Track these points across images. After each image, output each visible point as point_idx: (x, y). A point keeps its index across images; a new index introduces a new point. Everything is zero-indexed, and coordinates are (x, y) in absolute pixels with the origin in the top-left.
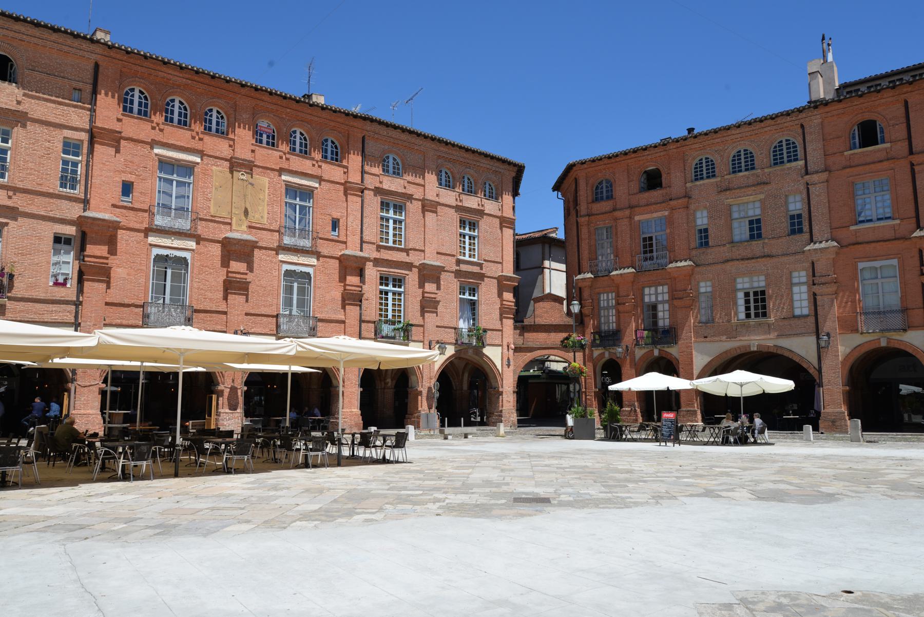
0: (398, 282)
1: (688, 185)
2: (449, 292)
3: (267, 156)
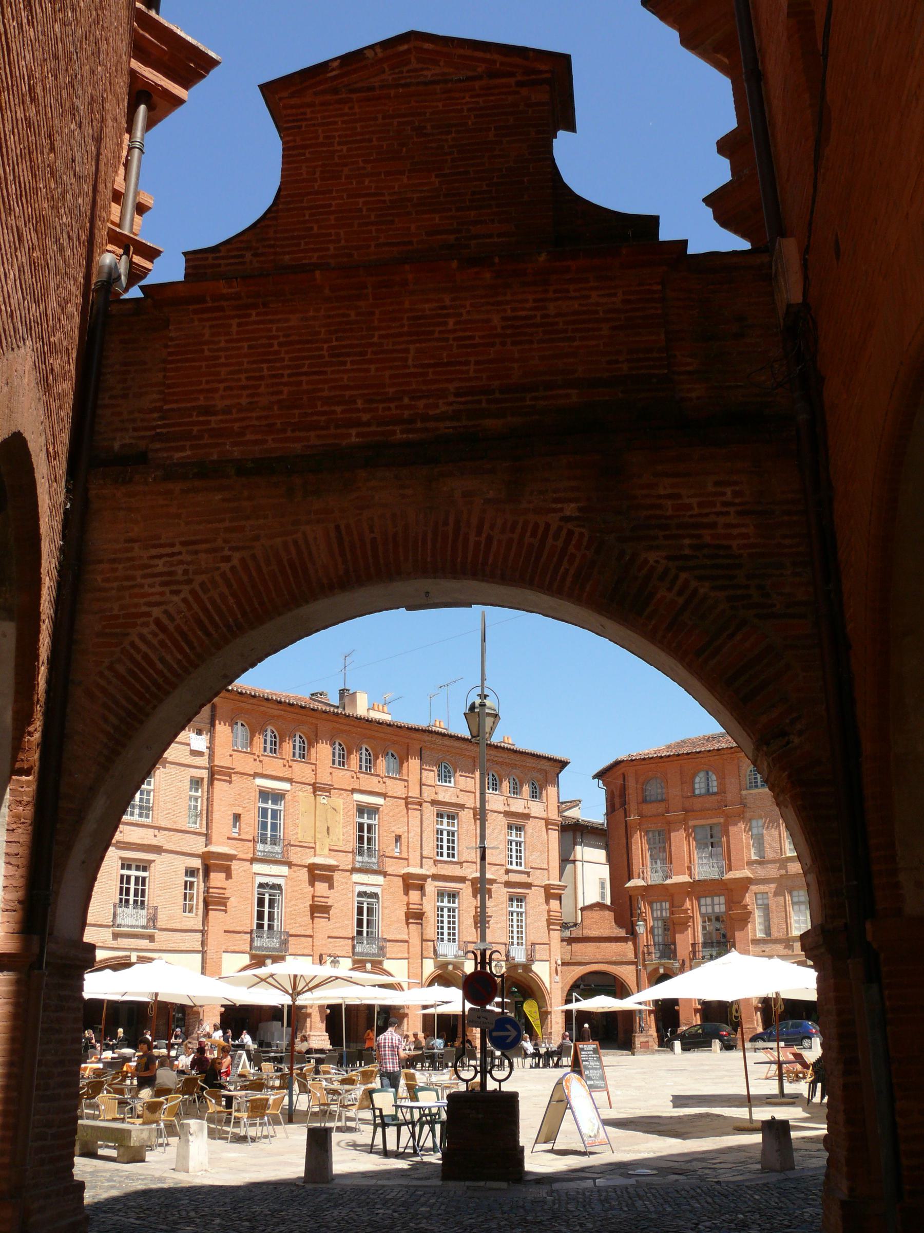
0: (453, 896)
1: (744, 792)
3: (342, 777)
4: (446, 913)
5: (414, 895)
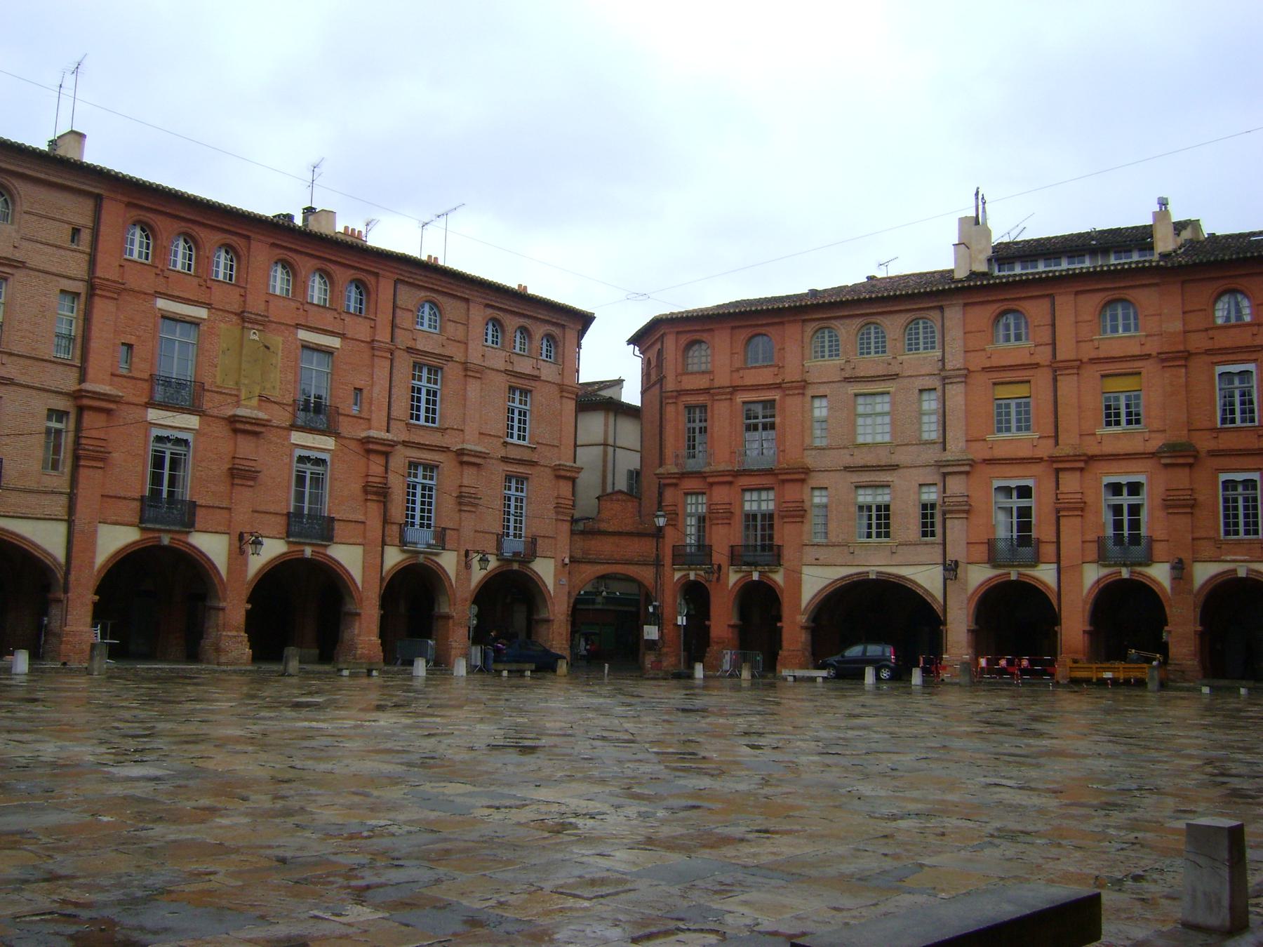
2: (489, 485)
4: (419, 491)
5: (376, 467)
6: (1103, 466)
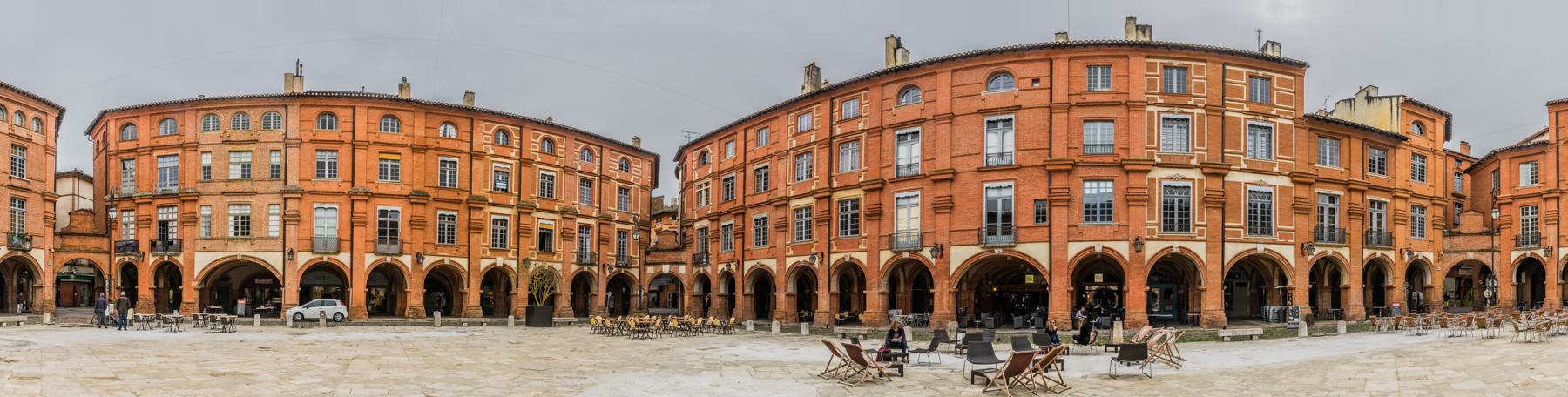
6: (376, 200)
